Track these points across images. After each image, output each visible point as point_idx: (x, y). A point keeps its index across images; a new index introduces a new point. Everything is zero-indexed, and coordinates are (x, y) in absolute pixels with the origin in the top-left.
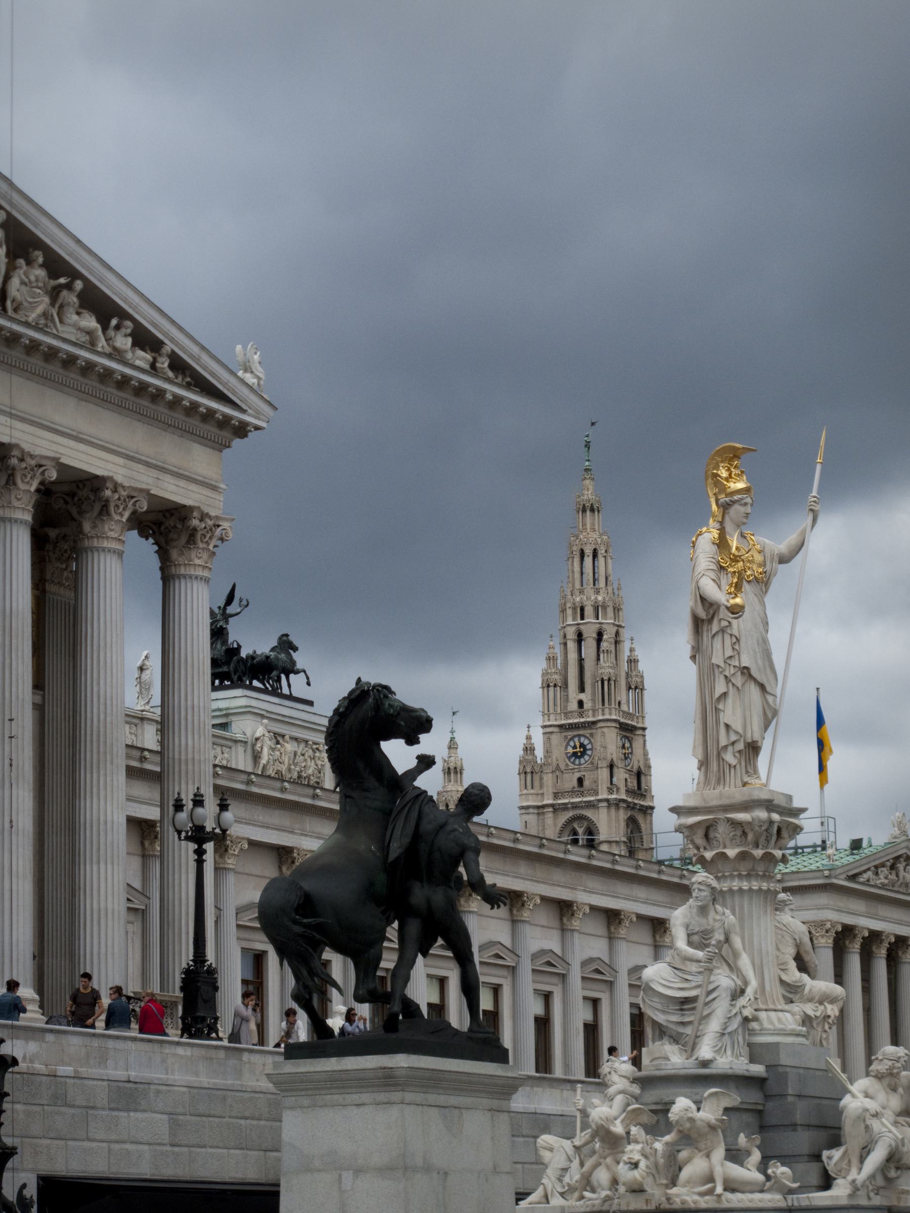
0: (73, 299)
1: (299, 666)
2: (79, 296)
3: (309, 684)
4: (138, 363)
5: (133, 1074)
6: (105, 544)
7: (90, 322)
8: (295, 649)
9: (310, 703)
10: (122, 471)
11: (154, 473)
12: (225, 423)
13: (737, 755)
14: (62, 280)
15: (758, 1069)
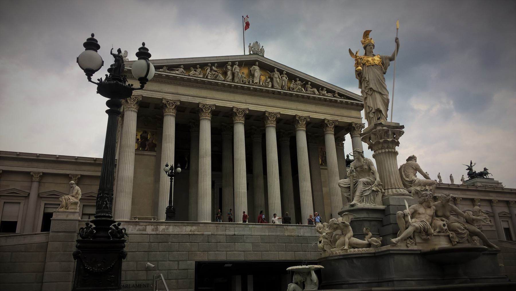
0: (309, 86)
1: (489, 173)
2: (310, 85)
3: (492, 175)
4: (329, 96)
5: (236, 233)
6: (328, 132)
7: (316, 90)
8: (488, 170)
9: (493, 179)
10: (330, 117)
11: (340, 117)
12: (357, 105)
13: (373, 114)
14: (304, 82)
15: (382, 207)
